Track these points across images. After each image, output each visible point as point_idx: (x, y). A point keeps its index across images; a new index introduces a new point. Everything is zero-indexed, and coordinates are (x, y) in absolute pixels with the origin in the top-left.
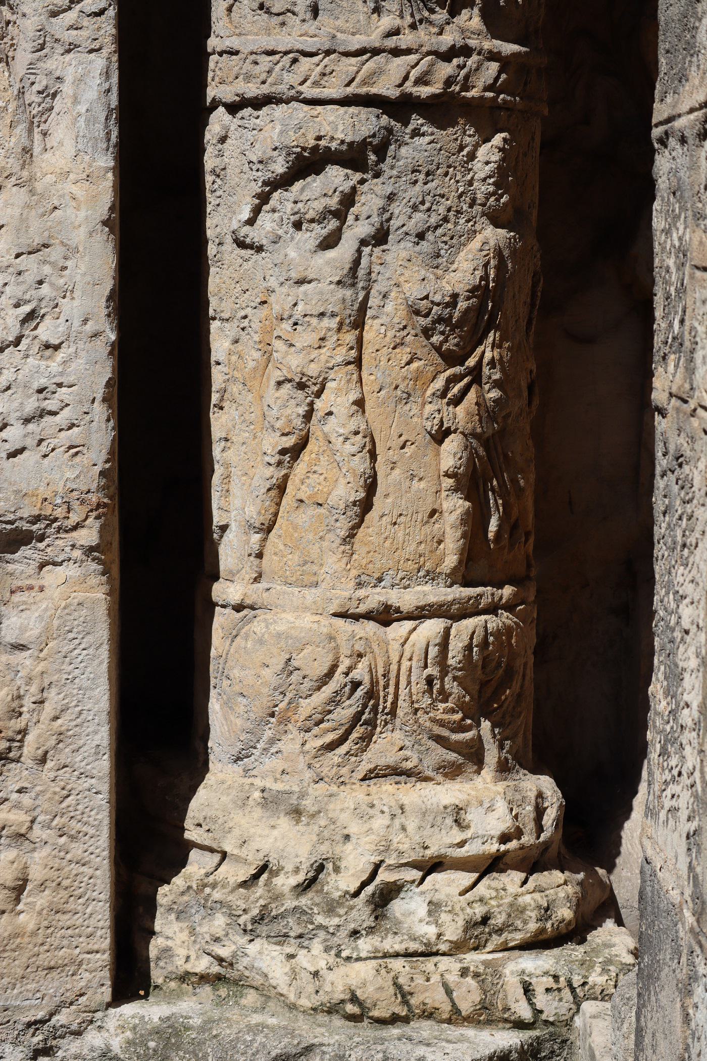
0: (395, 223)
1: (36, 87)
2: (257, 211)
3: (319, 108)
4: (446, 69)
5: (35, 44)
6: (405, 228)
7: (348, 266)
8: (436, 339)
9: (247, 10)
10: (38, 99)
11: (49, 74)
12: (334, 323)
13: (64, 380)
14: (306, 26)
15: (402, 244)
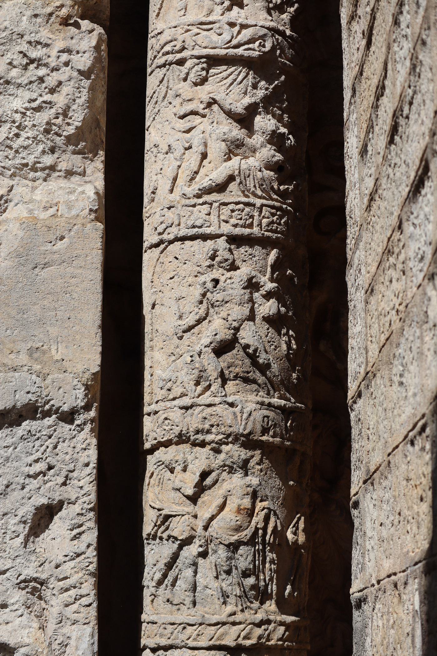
1: (57, 642)
3: (196, 652)
4: (258, 631)
5: (57, 620)
9: (161, 602)
10: (58, 647)
11: (64, 635)
14: (190, 611)
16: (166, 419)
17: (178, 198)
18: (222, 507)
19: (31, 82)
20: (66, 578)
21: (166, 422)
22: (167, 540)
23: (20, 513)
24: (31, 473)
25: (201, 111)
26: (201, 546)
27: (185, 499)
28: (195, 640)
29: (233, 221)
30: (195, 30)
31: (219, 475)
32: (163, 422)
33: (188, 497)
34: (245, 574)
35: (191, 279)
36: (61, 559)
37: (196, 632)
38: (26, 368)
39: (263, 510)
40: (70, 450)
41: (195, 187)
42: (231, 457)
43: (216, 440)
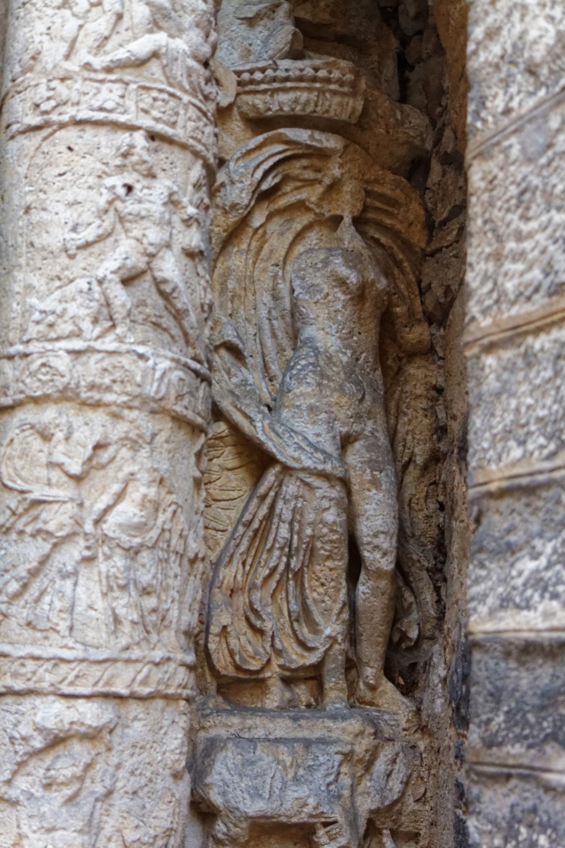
0: (119, 784)
2: (15, 773)
4: (157, 674)
6: (125, 789)
7: (87, 818)
15: (122, 801)
17: (77, 69)
18: (120, 497)
21: (44, 370)
22: (33, 536)
26: (88, 548)
27: (65, 479)
28: (72, 684)
31: (117, 451)
32: (39, 369)
34: (146, 592)
35: (92, 180)
37: (74, 673)
39: (170, 505)
41: (98, 62)
42: (138, 428)
43: (119, 401)
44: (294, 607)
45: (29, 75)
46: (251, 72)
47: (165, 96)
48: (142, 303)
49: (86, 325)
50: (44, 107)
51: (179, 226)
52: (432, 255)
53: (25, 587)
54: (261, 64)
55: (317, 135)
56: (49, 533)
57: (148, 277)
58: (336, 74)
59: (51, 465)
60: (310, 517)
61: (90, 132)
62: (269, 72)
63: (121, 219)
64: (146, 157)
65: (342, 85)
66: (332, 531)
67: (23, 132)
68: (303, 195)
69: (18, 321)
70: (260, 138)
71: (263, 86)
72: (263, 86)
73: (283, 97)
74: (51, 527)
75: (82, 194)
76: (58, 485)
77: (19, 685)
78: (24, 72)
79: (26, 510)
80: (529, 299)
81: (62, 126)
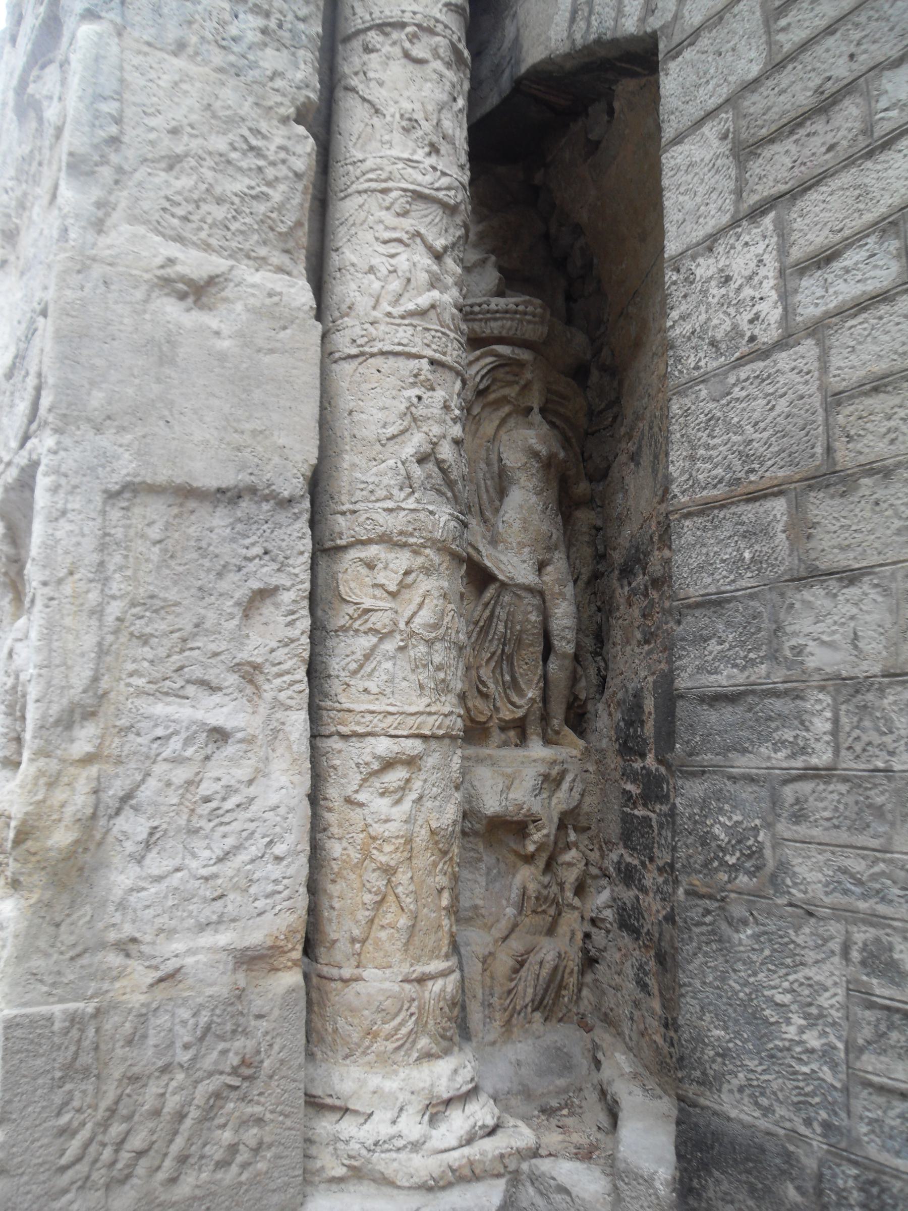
0: (426, 792)
1: (271, 727)
2: (361, 786)
8: (441, 846)
12: (402, 841)
13: (288, 875)
16: (368, 519)
18: (421, 606)
19: (250, 169)
20: (280, 663)
22: (365, 633)
23: (237, 595)
24: (249, 555)
25: (407, 241)
26: (402, 640)
27: (385, 595)
28: (396, 728)
29: (434, 346)
30: (401, 165)
31: (417, 576)
33: (390, 593)
34: (439, 668)
36: (274, 644)
38: (249, 450)
40: (286, 537)
44: (507, 678)
45: (346, 319)
46: (471, 306)
47: (439, 334)
48: (429, 477)
49: (395, 492)
50: (360, 341)
51: (450, 423)
52: (593, 434)
53: (361, 666)
54: (479, 301)
55: (517, 350)
56: (377, 631)
57: (432, 458)
58: (530, 309)
59: (376, 586)
60: (520, 617)
61: (392, 360)
62: (485, 306)
63: (415, 420)
64: (430, 377)
65: (534, 316)
66: (534, 627)
67: (344, 359)
68: (506, 391)
69: (347, 488)
70: (478, 353)
71: (480, 316)
72: (480, 316)
73: (493, 324)
74: (378, 626)
75: (389, 402)
76: (381, 599)
77: (360, 730)
78: (342, 317)
79: (360, 616)
80: (715, 486)
81: (372, 355)
